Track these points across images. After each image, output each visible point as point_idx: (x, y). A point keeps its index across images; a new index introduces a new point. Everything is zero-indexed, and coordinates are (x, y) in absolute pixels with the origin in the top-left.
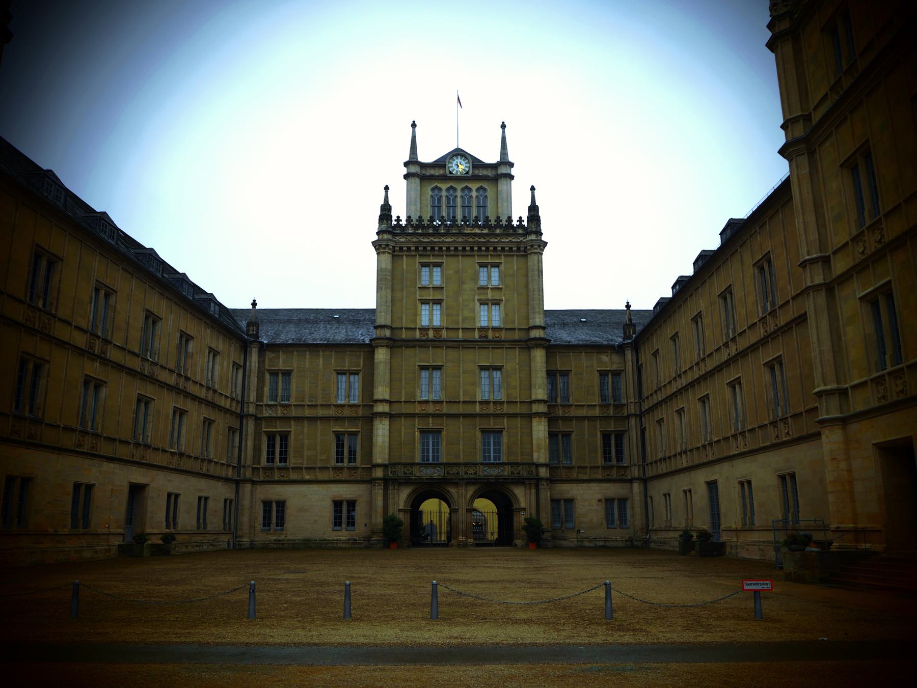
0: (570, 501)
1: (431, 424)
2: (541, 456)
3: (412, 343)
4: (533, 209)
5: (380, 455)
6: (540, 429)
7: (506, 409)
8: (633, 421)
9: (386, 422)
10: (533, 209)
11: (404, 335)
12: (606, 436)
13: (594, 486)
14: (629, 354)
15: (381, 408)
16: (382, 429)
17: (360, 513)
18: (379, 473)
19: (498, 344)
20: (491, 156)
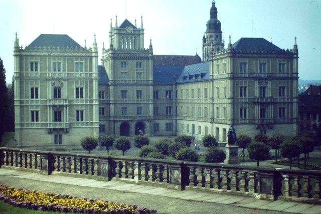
0: (158, 124)
1: (124, 106)
2: (151, 114)
3: (119, 84)
4: (151, 46)
5: (112, 114)
6: (151, 107)
7: (143, 102)
8: (174, 104)
9: (113, 105)
10: (151, 46)
11: (118, 82)
12: (167, 108)
13: (164, 121)
14: (174, 86)
15: (111, 102)
16: (112, 107)
17: (106, 127)
18: (112, 119)
19: (141, 84)
20: (139, 26)
